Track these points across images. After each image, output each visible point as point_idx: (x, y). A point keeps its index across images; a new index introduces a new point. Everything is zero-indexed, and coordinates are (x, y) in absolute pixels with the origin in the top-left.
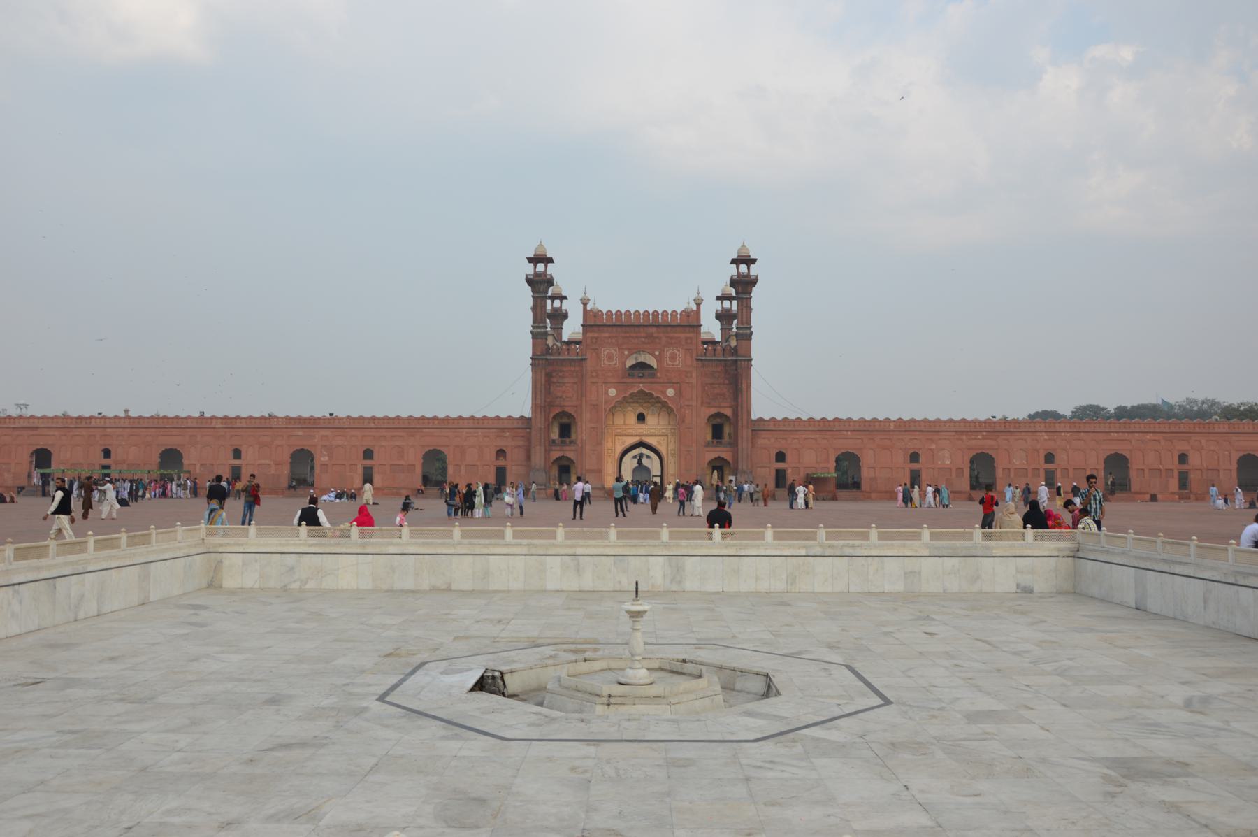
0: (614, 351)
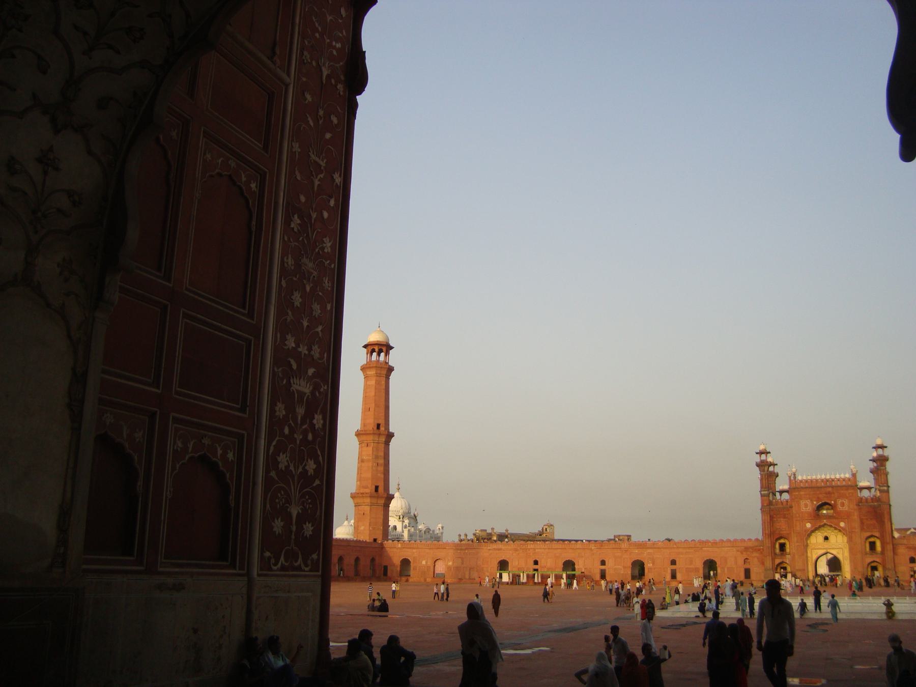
0: (808, 502)
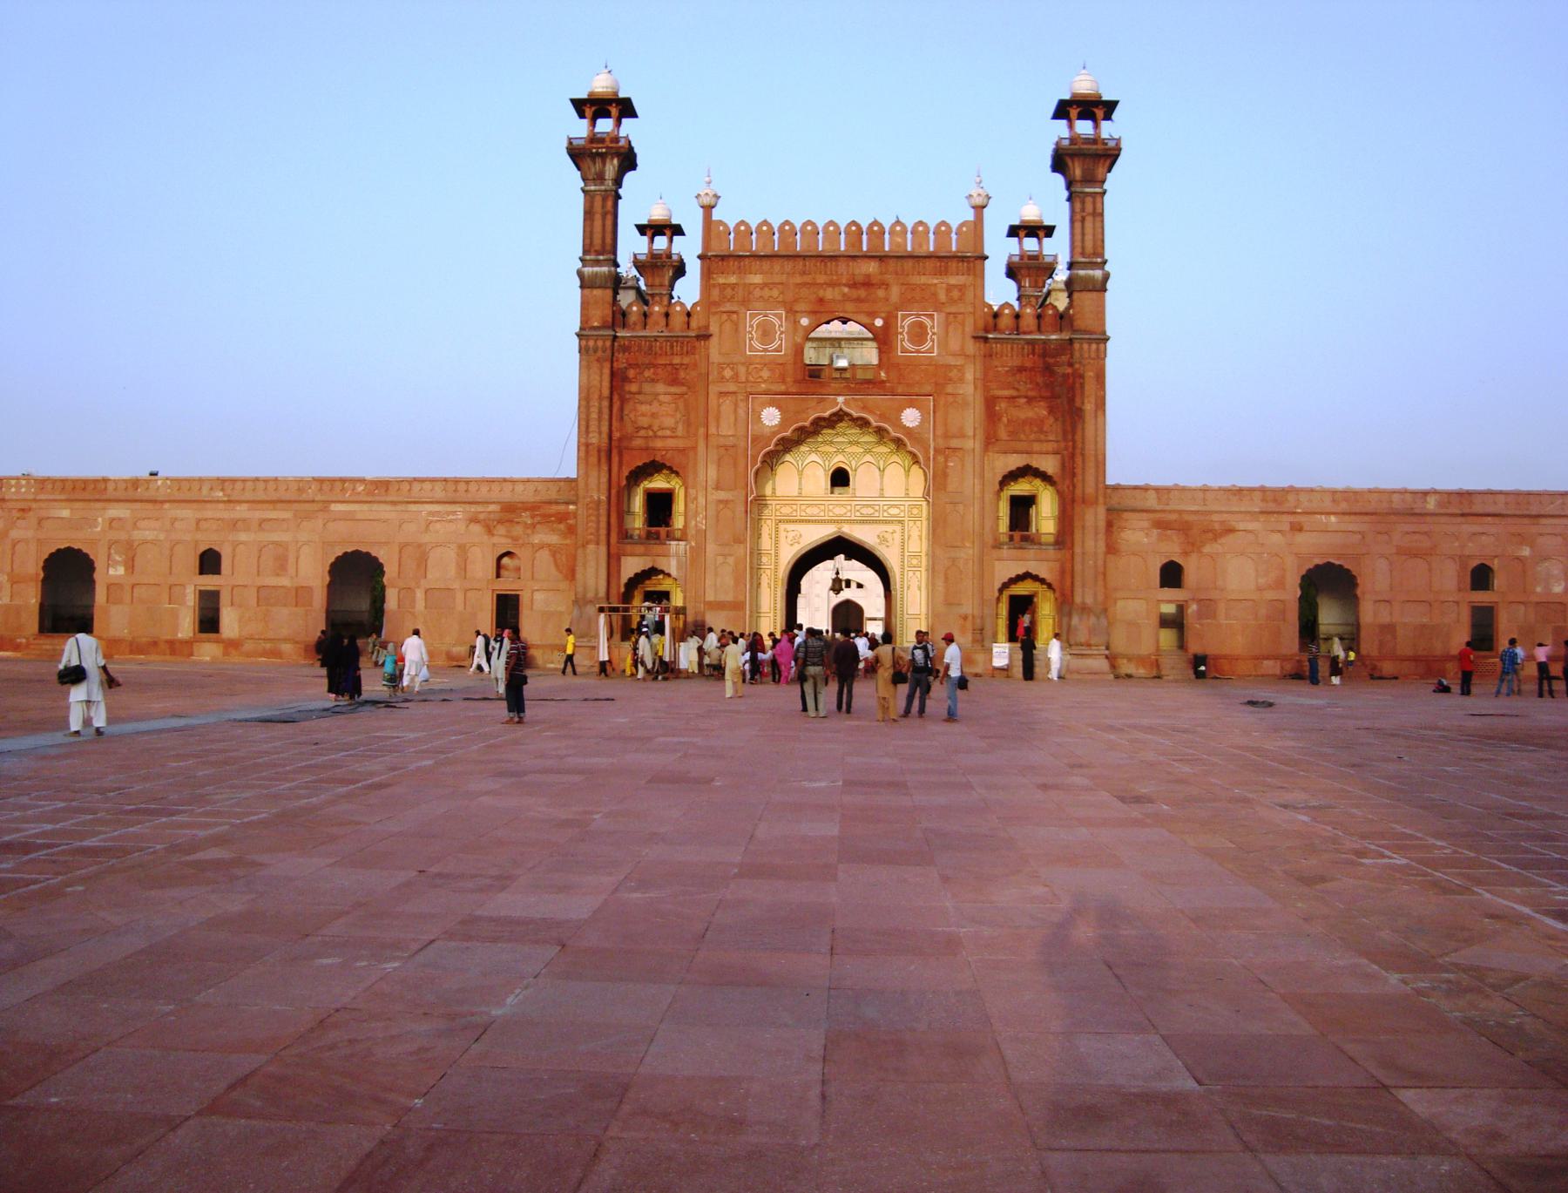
0: (777, 318)
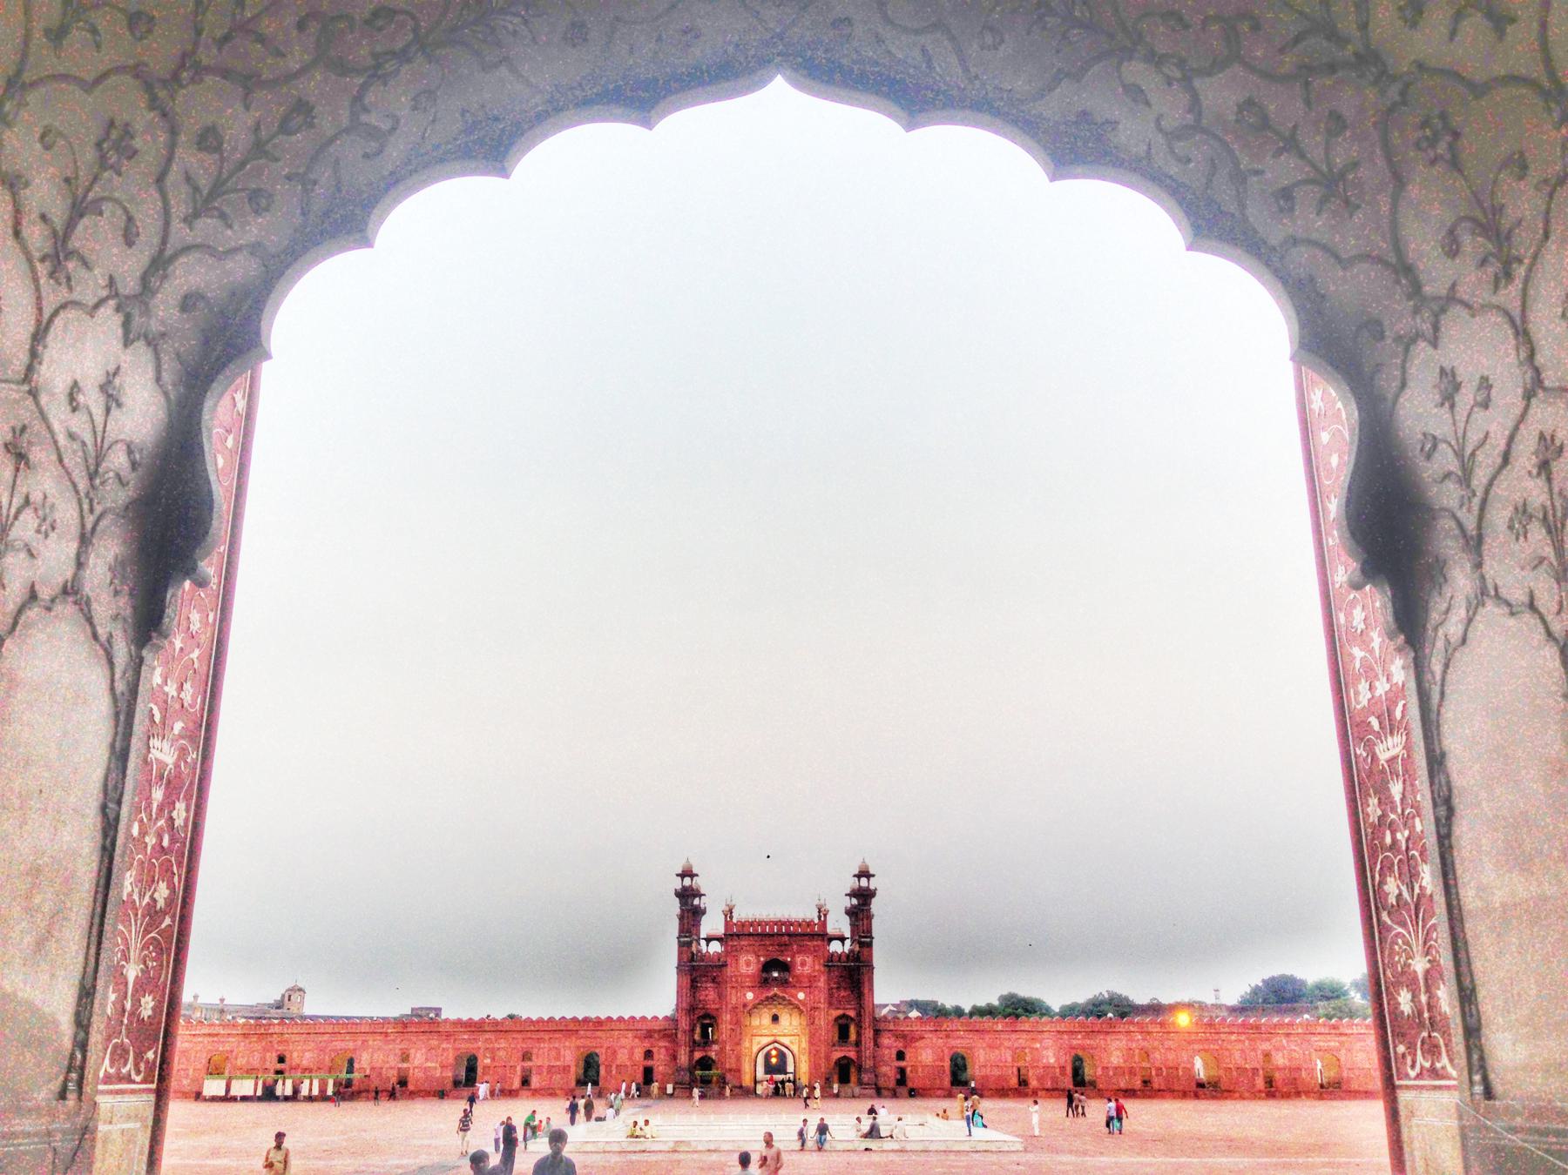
0: (751, 958)
